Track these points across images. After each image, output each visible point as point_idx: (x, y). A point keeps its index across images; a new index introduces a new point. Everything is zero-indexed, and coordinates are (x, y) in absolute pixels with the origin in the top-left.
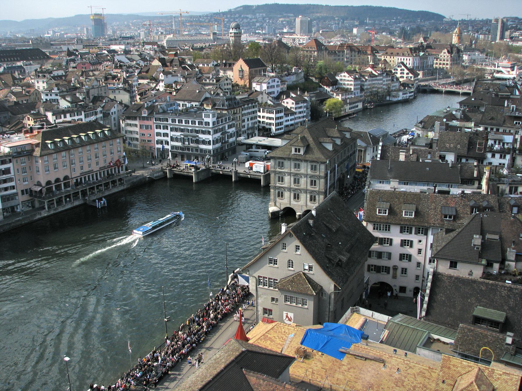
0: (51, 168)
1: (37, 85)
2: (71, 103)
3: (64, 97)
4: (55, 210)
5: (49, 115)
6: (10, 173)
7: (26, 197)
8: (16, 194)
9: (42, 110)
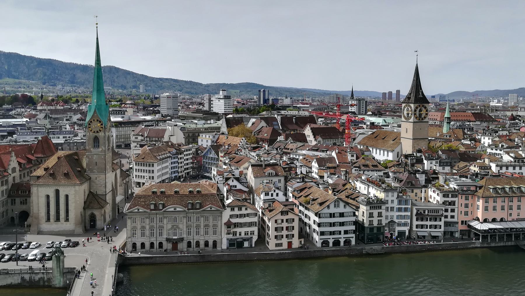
0: (490, 208)
1: (483, 141)
2: (515, 158)
3: (508, 153)
4: (488, 244)
5: (493, 166)
6: (454, 205)
7: (464, 227)
8: (457, 223)
9: (487, 161)
